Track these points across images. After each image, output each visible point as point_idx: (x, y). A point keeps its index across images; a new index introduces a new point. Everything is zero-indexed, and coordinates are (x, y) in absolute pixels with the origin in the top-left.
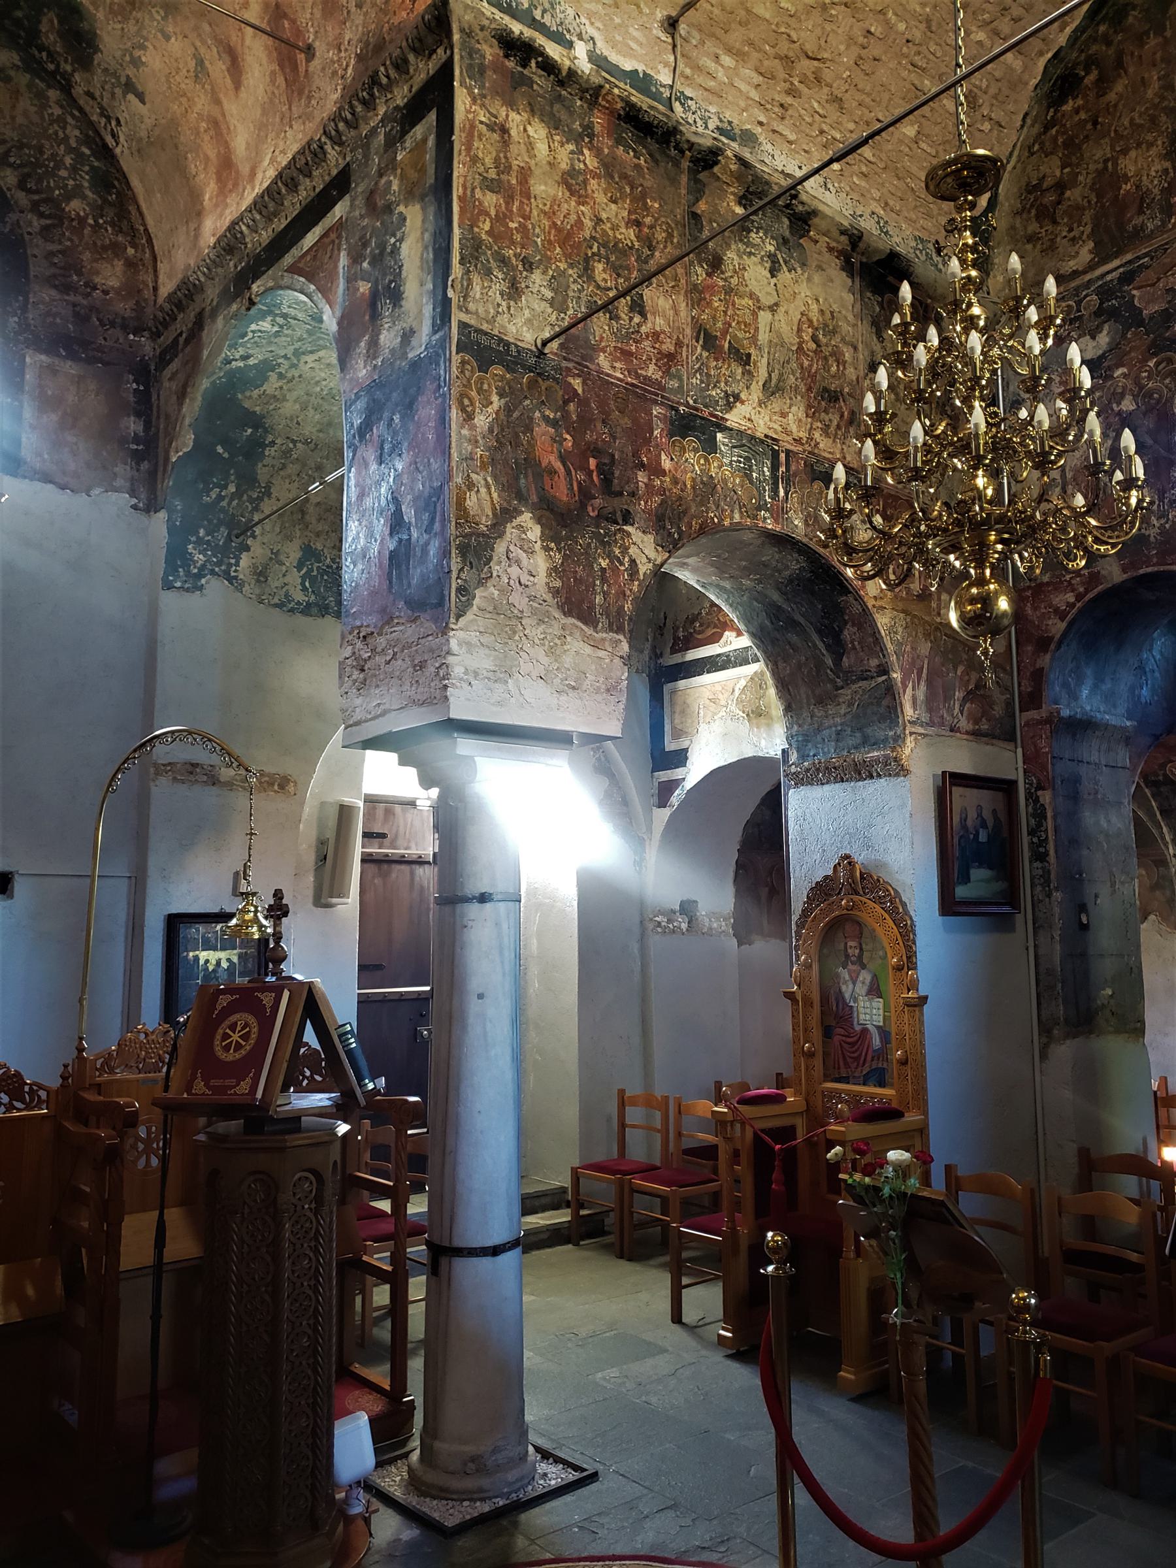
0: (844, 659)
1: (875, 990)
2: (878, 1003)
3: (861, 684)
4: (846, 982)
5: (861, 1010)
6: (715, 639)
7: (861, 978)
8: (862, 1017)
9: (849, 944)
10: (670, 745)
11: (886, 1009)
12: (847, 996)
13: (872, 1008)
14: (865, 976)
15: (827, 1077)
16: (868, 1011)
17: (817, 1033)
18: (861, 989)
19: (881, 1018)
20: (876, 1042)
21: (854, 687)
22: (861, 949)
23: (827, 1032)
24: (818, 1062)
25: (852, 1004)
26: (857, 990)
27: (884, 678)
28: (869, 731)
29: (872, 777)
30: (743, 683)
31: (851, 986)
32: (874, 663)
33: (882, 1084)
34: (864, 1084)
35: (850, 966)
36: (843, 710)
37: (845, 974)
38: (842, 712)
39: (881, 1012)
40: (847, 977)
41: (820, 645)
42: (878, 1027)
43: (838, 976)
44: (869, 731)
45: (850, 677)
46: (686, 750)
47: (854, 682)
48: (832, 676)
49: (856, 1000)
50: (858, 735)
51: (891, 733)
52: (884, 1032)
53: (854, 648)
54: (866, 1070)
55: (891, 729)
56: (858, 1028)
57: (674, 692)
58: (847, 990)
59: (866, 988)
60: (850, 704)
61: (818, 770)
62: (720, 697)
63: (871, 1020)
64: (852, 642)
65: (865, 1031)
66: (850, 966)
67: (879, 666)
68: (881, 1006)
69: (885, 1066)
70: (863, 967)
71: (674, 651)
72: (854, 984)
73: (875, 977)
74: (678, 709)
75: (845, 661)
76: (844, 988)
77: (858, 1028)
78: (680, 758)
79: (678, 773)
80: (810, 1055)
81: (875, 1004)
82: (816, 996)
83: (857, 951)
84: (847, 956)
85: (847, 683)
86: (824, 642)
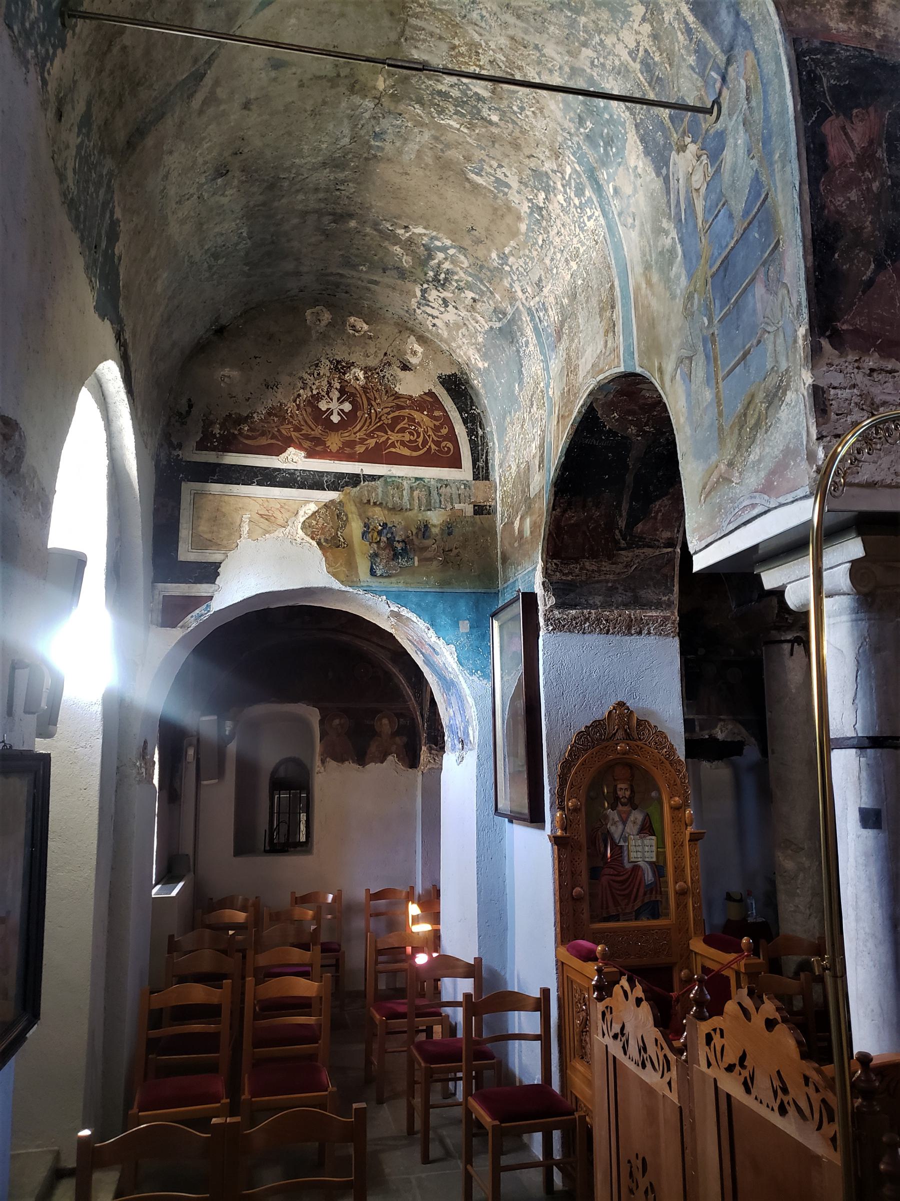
0: (640, 525)
1: (647, 829)
2: (651, 841)
3: (646, 550)
4: (614, 823)
5: (632, 848)
6: (277, 451)
7: (632, 818)
8: (633, 855)
9: (619, 786)
10: (186, 553)
11: (661, 844)
12: (617, 836)
13: (644, 845)
14: (637, 816)
15: (594, 919)
16: (640, 849)
17: (584, 877)
18: (632, 829)
19: (654, 854)
20: (649, 877)
21: (637, 551)
22: (632, 791)
23: (594, 873)
24: (585, 906)
25: (622, 843)
26: (628, 829)
27: (670, 550)
28: (642, 593)
29: (640, 633)
30: (312, 508)
31: (621, 827)
32: (667, 535)
33: (655, 915)
34: (636, 919)
35: (620, 807)
36: (618, 568)
37: (613, 815)
38: (618, 571)
39: (654, 848)
40: (617, 818)
41: (625, 506)
42: (651, 863)
43: (606, 817)
44: (642, 593)
45: (636, 541)
46: (218, 565)
47: (638, 547)
48: (618, 535)
49: (626, 840)
50: (629, 594)
51: (665, 598)
52: (658, 868)
53: (655, 518)
54: (638, 904)
55: (664, 595)
56: (628, 866)
57: (198, 495)
58: (616, 831)
59: (637, 827)
60: (628, 566)
61: (587, 619)
62: (278, 514)
63: (643, 857)
64: (657, 513)
65: (636, 868)
66: (620, 807)
67: (669, 539)
68: (654, 843)
69: (659, 898)
70: (635, 808)
71: (202, 446)
72: (624, 823)
73: (647, 818)
74: (205, 515)
75: (639, 527)
76: (613, 829)
77: (628, 866)
78: (209, 572)
79: (202, 589)
80: (577, 899)
81: (647, 842)
82: (583, 838)
83: (628, 793)
84: (617, 799)
85: (629, 547)
86: (631, 504)
